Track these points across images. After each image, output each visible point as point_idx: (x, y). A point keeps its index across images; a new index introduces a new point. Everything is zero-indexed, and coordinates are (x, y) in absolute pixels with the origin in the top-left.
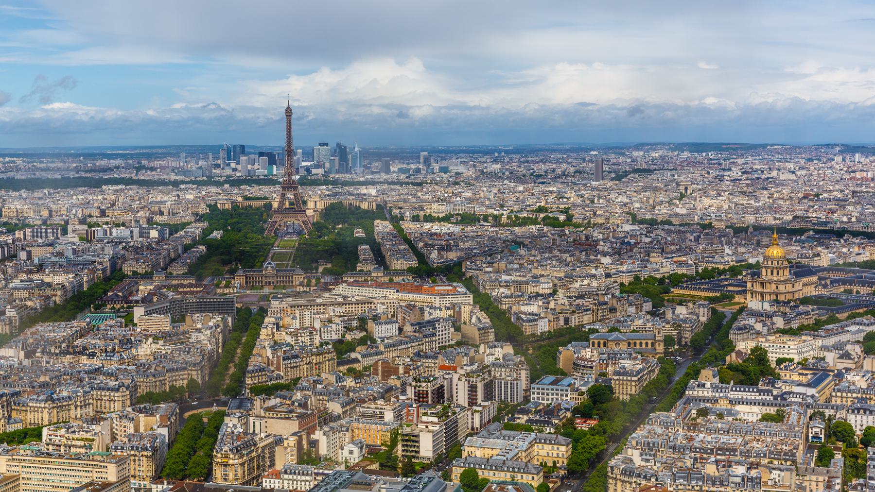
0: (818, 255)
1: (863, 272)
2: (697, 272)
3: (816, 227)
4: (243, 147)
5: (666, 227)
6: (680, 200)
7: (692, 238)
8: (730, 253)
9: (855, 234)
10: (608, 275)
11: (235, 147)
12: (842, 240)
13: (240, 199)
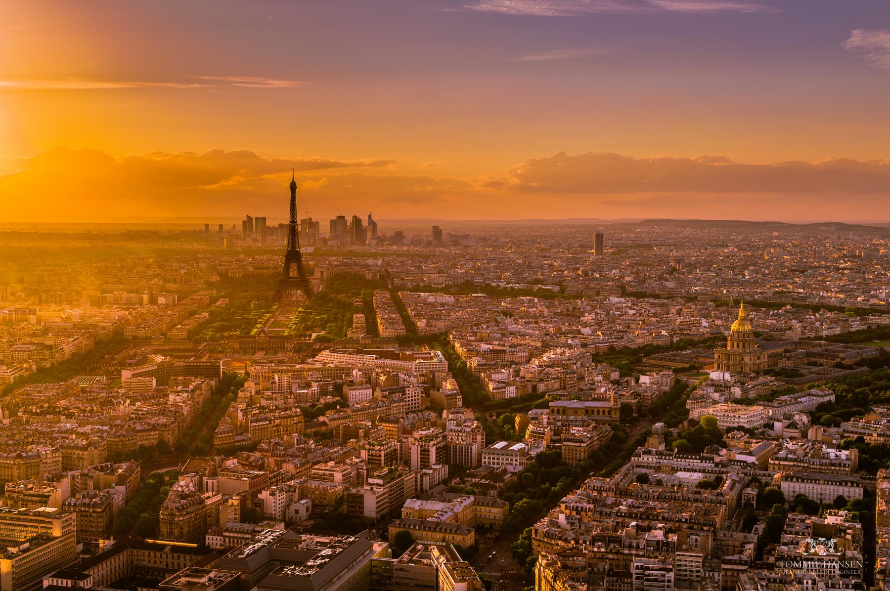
0: (790, 329)
1: (829, 345)
2: (672, 342)
3: (796, 302)
4: (264, 219)
5: (651, 300)
6: (671, 274)
7: (675, 311)
8: (707, 325)
9: (830, 309)
10: (584, 345)
11: (257, 218)
12: (818, 316)
13: (251, 268)
